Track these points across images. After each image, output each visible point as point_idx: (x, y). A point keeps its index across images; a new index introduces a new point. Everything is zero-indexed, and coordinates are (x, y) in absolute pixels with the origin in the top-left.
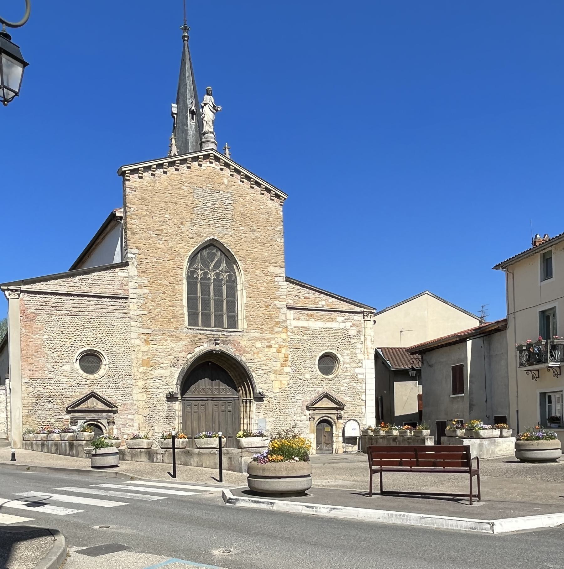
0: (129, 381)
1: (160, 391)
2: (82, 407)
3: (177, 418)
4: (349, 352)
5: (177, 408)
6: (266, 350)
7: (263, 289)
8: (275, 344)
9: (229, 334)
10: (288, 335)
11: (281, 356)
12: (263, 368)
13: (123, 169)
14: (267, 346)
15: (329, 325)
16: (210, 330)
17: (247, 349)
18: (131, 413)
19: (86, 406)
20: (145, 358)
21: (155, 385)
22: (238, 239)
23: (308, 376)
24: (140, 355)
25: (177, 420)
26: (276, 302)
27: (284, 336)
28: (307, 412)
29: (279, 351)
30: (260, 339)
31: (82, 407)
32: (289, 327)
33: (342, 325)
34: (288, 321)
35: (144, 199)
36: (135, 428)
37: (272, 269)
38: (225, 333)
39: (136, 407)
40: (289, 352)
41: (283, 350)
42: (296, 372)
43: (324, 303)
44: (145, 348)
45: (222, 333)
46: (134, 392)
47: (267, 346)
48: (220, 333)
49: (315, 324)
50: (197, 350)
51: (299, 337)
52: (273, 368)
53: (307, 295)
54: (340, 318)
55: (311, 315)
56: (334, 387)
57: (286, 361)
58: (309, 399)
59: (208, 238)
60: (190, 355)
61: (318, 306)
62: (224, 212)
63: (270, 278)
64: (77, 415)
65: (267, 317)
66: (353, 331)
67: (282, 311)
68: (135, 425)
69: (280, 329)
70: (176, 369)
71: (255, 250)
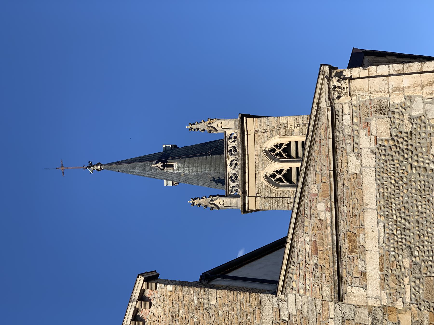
10: (405, 310)
15: (370, 195)
32: (385, 301)
33: (369, 160)
34: (371, 302)
43: (321, 207)
49: (373, 233)
51: (406, 280)
53: (308, 248)
54: (352, 165)
55: (352, 241)
61: (329, 222)
66: (381, 127)
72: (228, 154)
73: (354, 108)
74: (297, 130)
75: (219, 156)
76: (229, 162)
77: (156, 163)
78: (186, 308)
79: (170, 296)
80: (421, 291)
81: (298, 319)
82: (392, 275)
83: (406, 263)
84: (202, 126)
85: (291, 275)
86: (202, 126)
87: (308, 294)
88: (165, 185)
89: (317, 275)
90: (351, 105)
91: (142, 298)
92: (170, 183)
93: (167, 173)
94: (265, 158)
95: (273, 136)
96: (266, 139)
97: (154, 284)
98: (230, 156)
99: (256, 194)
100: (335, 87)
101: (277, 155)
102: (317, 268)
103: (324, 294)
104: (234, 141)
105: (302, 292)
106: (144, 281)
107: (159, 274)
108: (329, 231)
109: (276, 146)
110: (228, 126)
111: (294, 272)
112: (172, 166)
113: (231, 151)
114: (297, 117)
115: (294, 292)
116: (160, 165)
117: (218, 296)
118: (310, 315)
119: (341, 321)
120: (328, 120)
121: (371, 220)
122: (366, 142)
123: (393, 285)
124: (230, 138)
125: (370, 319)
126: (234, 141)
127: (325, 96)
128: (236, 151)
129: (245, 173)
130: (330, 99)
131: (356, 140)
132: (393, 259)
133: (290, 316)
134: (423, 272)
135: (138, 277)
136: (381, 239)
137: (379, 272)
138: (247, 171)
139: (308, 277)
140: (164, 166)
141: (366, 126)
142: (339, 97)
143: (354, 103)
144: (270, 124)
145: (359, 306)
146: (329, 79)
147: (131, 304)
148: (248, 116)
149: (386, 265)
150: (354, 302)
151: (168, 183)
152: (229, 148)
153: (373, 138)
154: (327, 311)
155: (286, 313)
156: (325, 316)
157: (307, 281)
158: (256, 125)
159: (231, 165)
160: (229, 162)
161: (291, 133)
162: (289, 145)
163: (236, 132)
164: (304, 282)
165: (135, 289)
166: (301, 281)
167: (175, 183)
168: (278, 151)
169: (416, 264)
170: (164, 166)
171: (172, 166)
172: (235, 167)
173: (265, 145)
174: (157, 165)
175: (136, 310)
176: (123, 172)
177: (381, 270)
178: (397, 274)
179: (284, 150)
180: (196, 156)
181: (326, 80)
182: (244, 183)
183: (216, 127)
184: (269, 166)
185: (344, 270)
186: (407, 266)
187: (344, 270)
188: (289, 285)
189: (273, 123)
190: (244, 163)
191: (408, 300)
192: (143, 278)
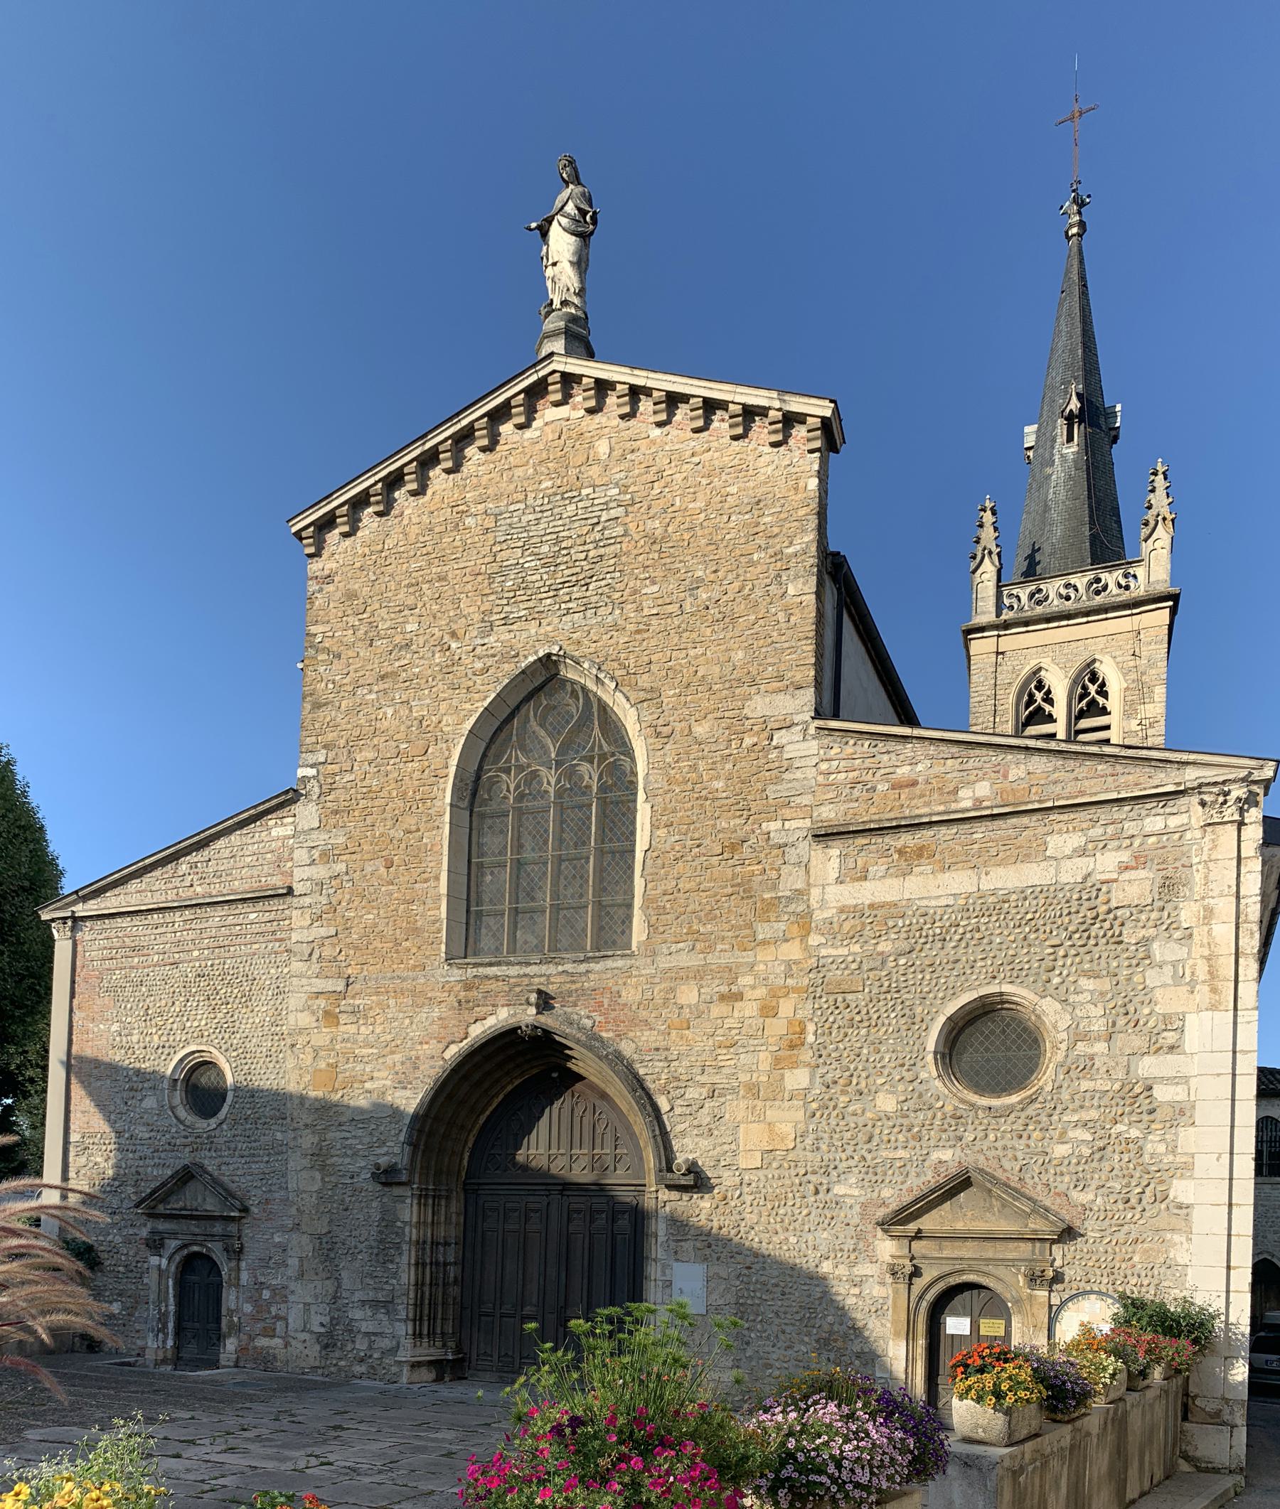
0: (279, 1136)
1: (363, 1164)
2: (176, 1204)
3: (405, 1247)
4: (1106, 984)
5: (407, 1219)
6: (717, 1010)
7: (719, 784)
8: (753, 987)
9: (583, 967)
10: (806, 948)
11: (777, 1027)
12: (703, 1079)
13: (294, 530)
14: (723, 998)
16: (519, 963)
17: (643, 1014)
18: (282, 1229)
19: (181, 1204)
20: (323, 1065)
21: (350, 1147)
22: (638, 632)
23: (886, 1103)
24: (307, 1059)
25: (406, 1254)
26: (773, 826)
27: (793, 951)
28: (887, 1248)
29: (769, 1011)
30: (698, 975)
31: (176, 1204)
32: (819, 916)
34: (815, 893)
35: (352, 595)
36: (290, 1272)
37: (759, 706)
38: (569, 967)
39: (293, 1211)
40: (805, 1011)
41: (786, 1008)
42: (838, 1088)
44: (321, 1038)
45: (560, 968)
46: (291, 1164)
47: (723, 998)
48: (551, 969)
50: (477, 1031)
51: (856, 948)
52: (744, 1077)
56: (1016, 1143)
57: (792, 1047)
58: (893, 1196)
59: (531, 659)
60: (453, 1049)
62: (591, 554)
63: (748, 741)
64: (162, 1226)
65: (730, 890)
67: (792, 854)
68: (290, 1262)
69: (782, 926)
70: (408, 1093)
71: (692, 653)
72: (1090, 576)
73: (1177, 836)
74: (1133, 724)
75: (1088, 554)
76: (1073, 580)
77: (1078, 394)
78: (776, 530)
79: (796, 489)
80: (839, 972)
81: (777, 764)
82: (863, 924)
83: (885, 947)
84: (1160, 501)
85: (852, 742)
86: (1160, 501)
87: (820, 779)
88: (1027, 429)
89: (856, 793)
90: (1182, 830)
91: (790, 420)
92: (1030, 441)
93: (1055, 428)
94: (1078, 663)
95: (1125, 675)
96: (1118, 659)
97: (818, 444)
98: (1086, 580)
99: (1002, 653)
100: (1226, 794)
101: (1085, 688)
102: (867, 791)
103: (823, 809)
104: (1120, 586)
105: (824, 766)
106: (823, 418)
107: (837, 452)
108: (936, 808)
109: (1103, 684)
110: (1155, 565)
111: (858, 748)
112: (1070, 439)
113: (1098, 580)
114: (1163, 723)
115: (822, 752)
116: (1074, 405)
117: (804, 598)
118: (785, 786)
119: (781, 841)
120: (1157, 787)
121: (959, 882)
122: (1107, 863)
123: (846, 926)
124: (1126, 576)
125: (788, 893)
126: (1120, 586)
127: (1209, 775)
128: (1098, 593)
129: (1048, 620)
130: (1200, 786)
131: (1112, 845)
132: (891, 923)
133: (779, 748)
134: (871, 974)
135: (831, 401)
136: (925, 903)
137: (867, 902)
138: (1051, 625)
139: (851, 775)
140: (1070, 419)
141: (1140, 861)
142: (1203, 804)
143: (1188, 835)
144: (1151, 664)
145: (808, 872)
146: (1243, 780)
147: (774, 394)
148: (1174, 611)
149: (880, 913)
150: (813, 863)
151: (1030, 434)
152: (1104, 576)
153: (1115, 876)
154: (794, 815)
155: (784, 741)
156: (787, 812)
157: (843, 775)
158: (1152, 632)
159: (1067, 586)
160: (1072, 582)
161: (1128, 714)
162: (1104, 711)
163: (1139, 589)
164: (841, 768)
165: (806, 400)
166: (843, 763)
167: (1031, 453)
168: (1093, 689)
169: (883, 962)
170: (1070, 419)
171: (1070, 439)
172: (1061, 596)
173: (1107, 659)
174: (1074, 397)
175: (763, 411)
176: (1061, 304)
177: (871, 906)
178: (866, 933)
179: (1093, 702)
180: (1089, 497)
181: (1243, 773)
182: (1026, 623)
183: (1155, 536)
184: (1061, 674)
185: (867, 841)
186: (880, 948)
187: (867, 841)
188: (834, 741)
189: (1154, 671)
190: (1068, 616)
191: (824, 952)
192: (828, 413)
